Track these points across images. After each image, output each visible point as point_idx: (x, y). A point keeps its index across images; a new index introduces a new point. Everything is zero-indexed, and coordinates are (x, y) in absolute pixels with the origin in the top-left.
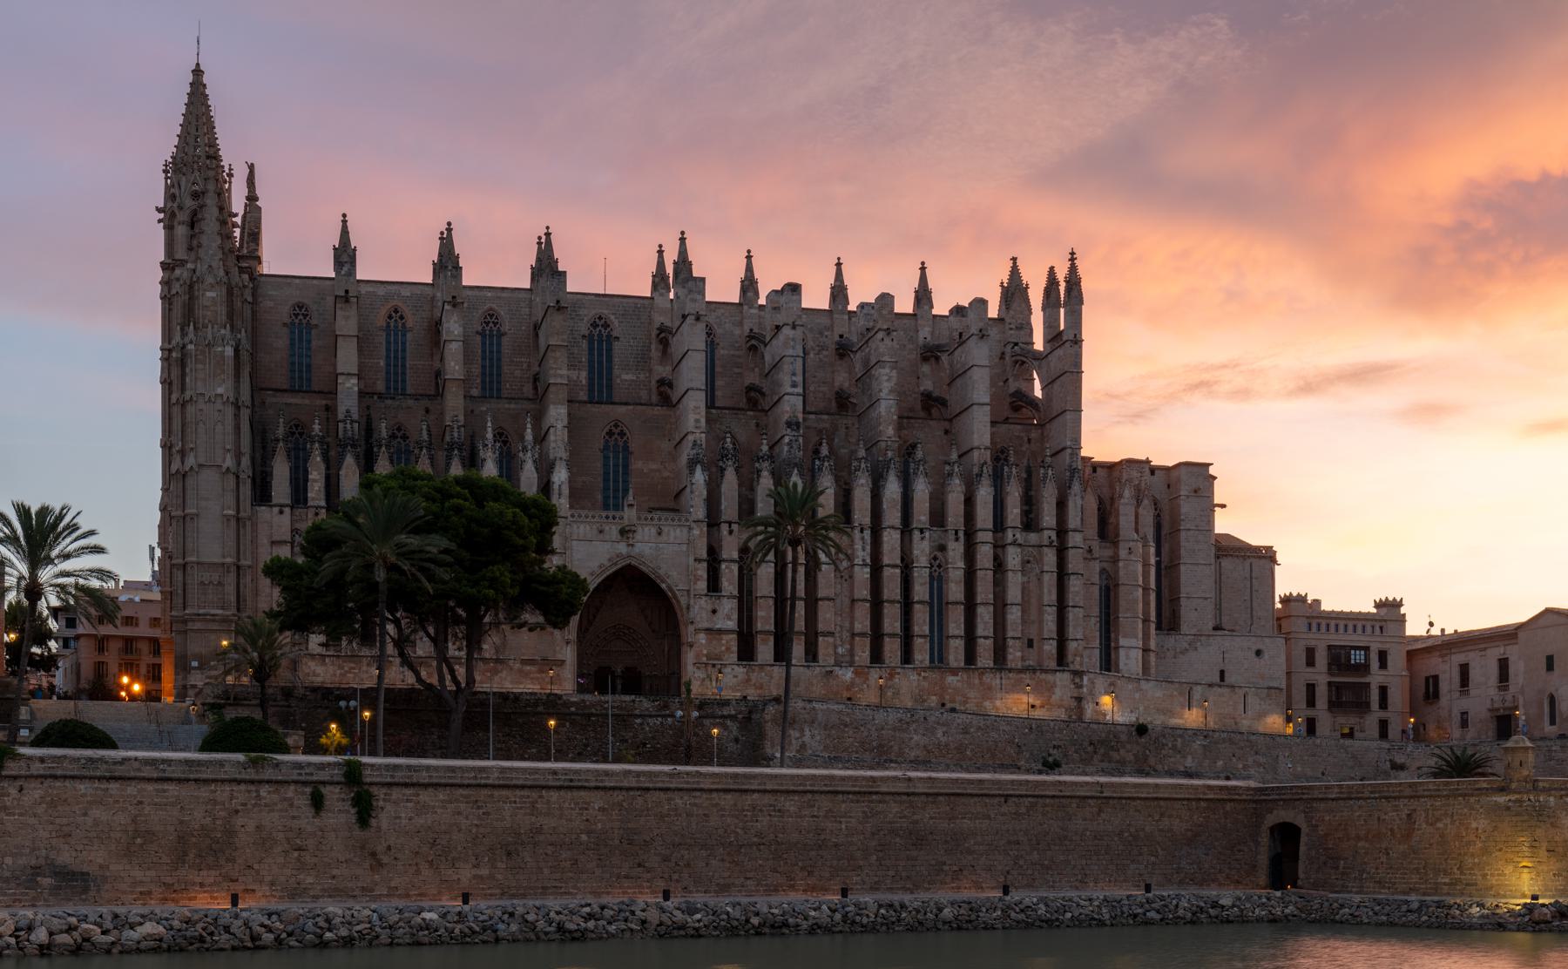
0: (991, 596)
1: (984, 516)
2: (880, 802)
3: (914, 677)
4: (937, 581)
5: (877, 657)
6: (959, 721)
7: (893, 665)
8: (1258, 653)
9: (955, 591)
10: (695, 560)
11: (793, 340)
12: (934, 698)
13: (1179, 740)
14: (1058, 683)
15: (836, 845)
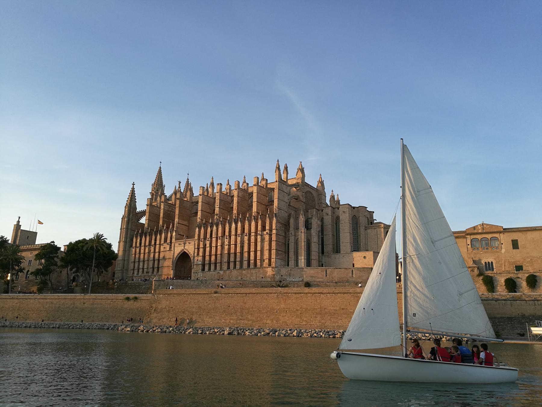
0: (254, 249)
1: (253, 229)
2: (76, 301)
3: (236, 272)
4: (242, 247)
5: (229, 268)
6: (216, 283)
7: (232, 269)
8: (365, 257)
9: (246, 249)
10: (195, 249)
11: (218, 196)
12: (240, 277)
13: (296, 285)
14: (268, 271)
15: (62, 311)
